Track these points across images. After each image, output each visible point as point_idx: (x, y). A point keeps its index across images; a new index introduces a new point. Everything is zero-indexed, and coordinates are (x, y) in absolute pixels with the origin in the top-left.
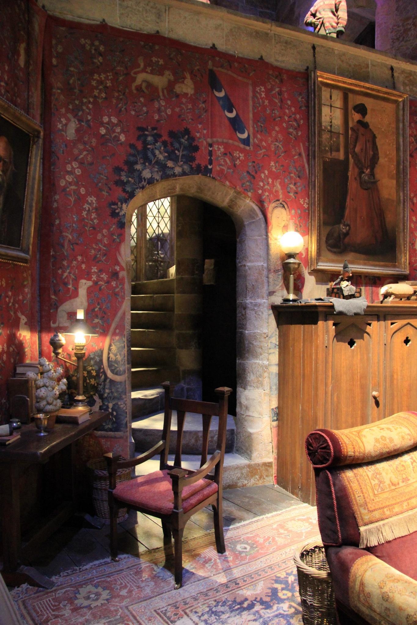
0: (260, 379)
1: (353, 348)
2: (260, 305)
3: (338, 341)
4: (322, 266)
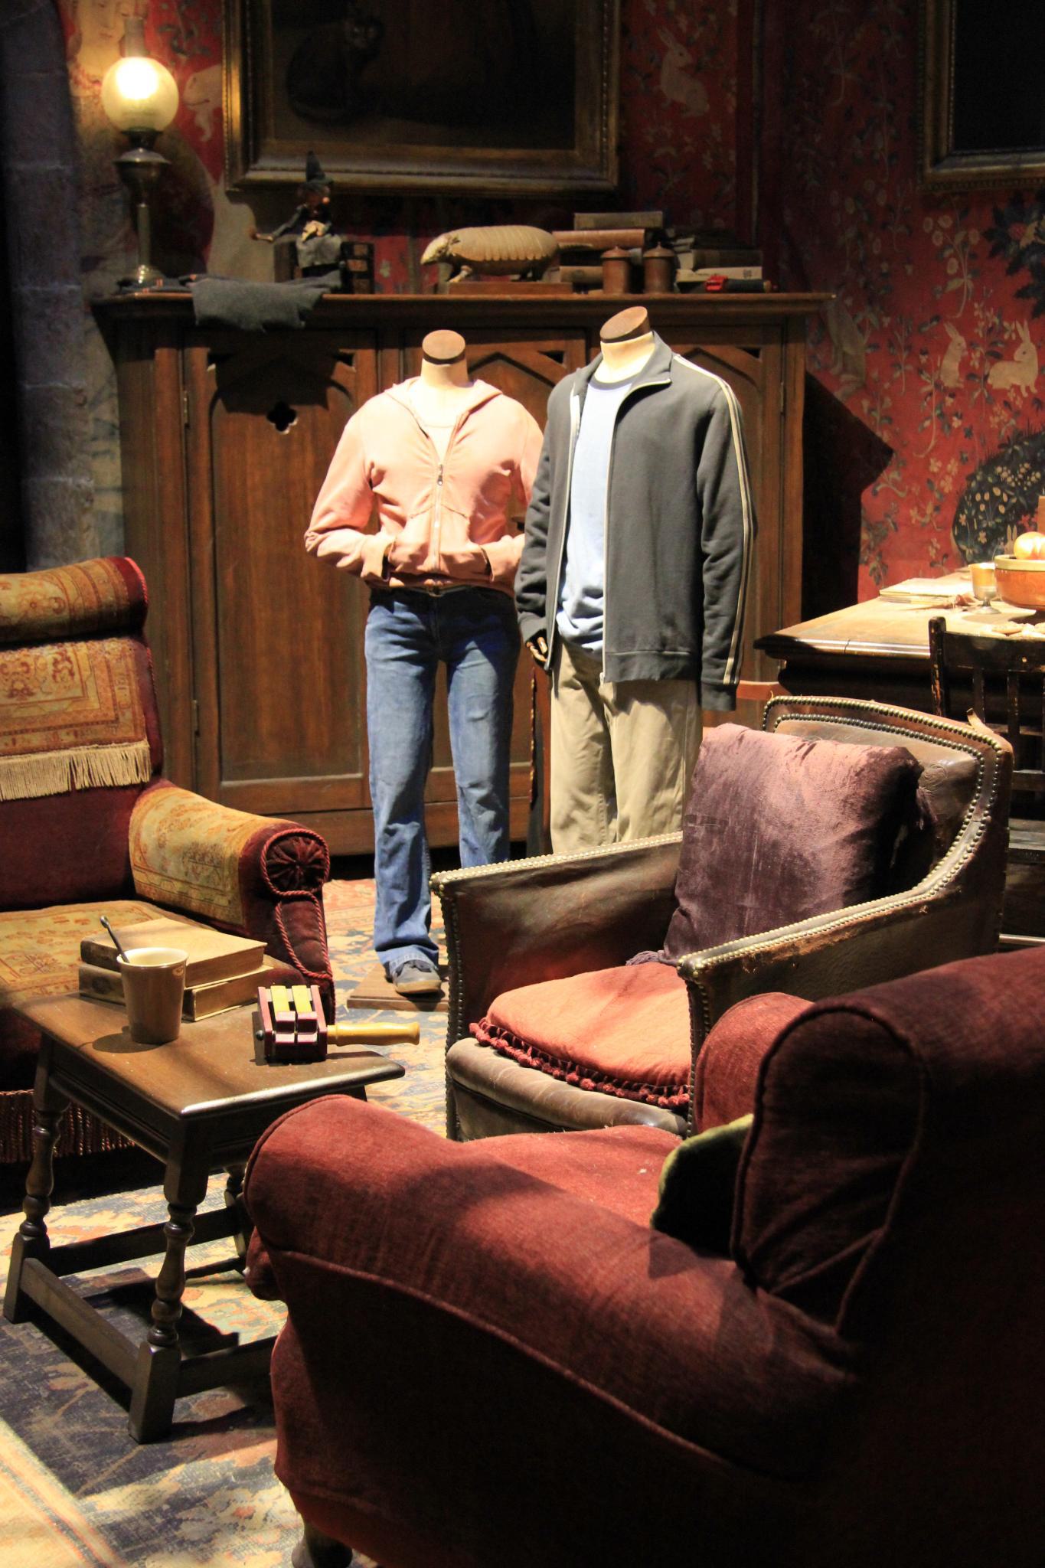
0: (72, 534)
1: (287, 432)
2: (56, 300)
3: (230, 409)
4: (266, 171)
